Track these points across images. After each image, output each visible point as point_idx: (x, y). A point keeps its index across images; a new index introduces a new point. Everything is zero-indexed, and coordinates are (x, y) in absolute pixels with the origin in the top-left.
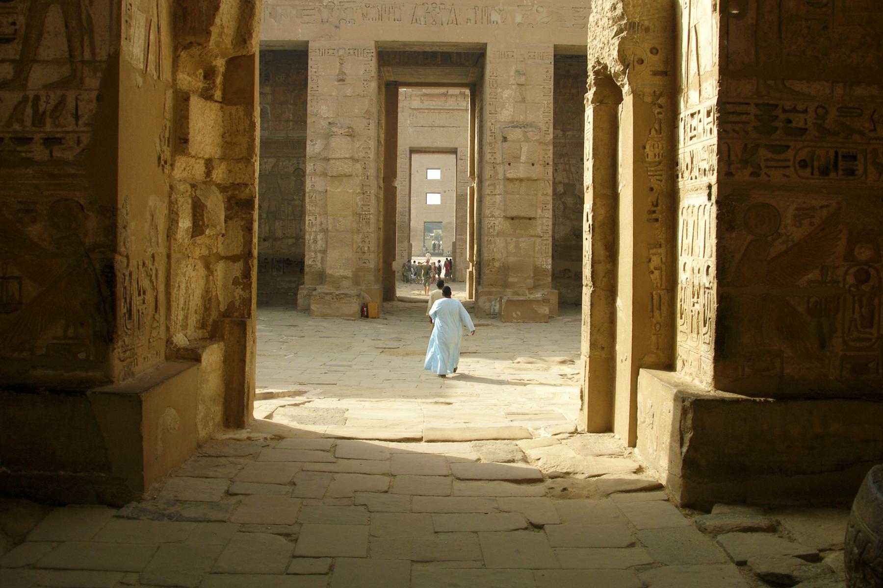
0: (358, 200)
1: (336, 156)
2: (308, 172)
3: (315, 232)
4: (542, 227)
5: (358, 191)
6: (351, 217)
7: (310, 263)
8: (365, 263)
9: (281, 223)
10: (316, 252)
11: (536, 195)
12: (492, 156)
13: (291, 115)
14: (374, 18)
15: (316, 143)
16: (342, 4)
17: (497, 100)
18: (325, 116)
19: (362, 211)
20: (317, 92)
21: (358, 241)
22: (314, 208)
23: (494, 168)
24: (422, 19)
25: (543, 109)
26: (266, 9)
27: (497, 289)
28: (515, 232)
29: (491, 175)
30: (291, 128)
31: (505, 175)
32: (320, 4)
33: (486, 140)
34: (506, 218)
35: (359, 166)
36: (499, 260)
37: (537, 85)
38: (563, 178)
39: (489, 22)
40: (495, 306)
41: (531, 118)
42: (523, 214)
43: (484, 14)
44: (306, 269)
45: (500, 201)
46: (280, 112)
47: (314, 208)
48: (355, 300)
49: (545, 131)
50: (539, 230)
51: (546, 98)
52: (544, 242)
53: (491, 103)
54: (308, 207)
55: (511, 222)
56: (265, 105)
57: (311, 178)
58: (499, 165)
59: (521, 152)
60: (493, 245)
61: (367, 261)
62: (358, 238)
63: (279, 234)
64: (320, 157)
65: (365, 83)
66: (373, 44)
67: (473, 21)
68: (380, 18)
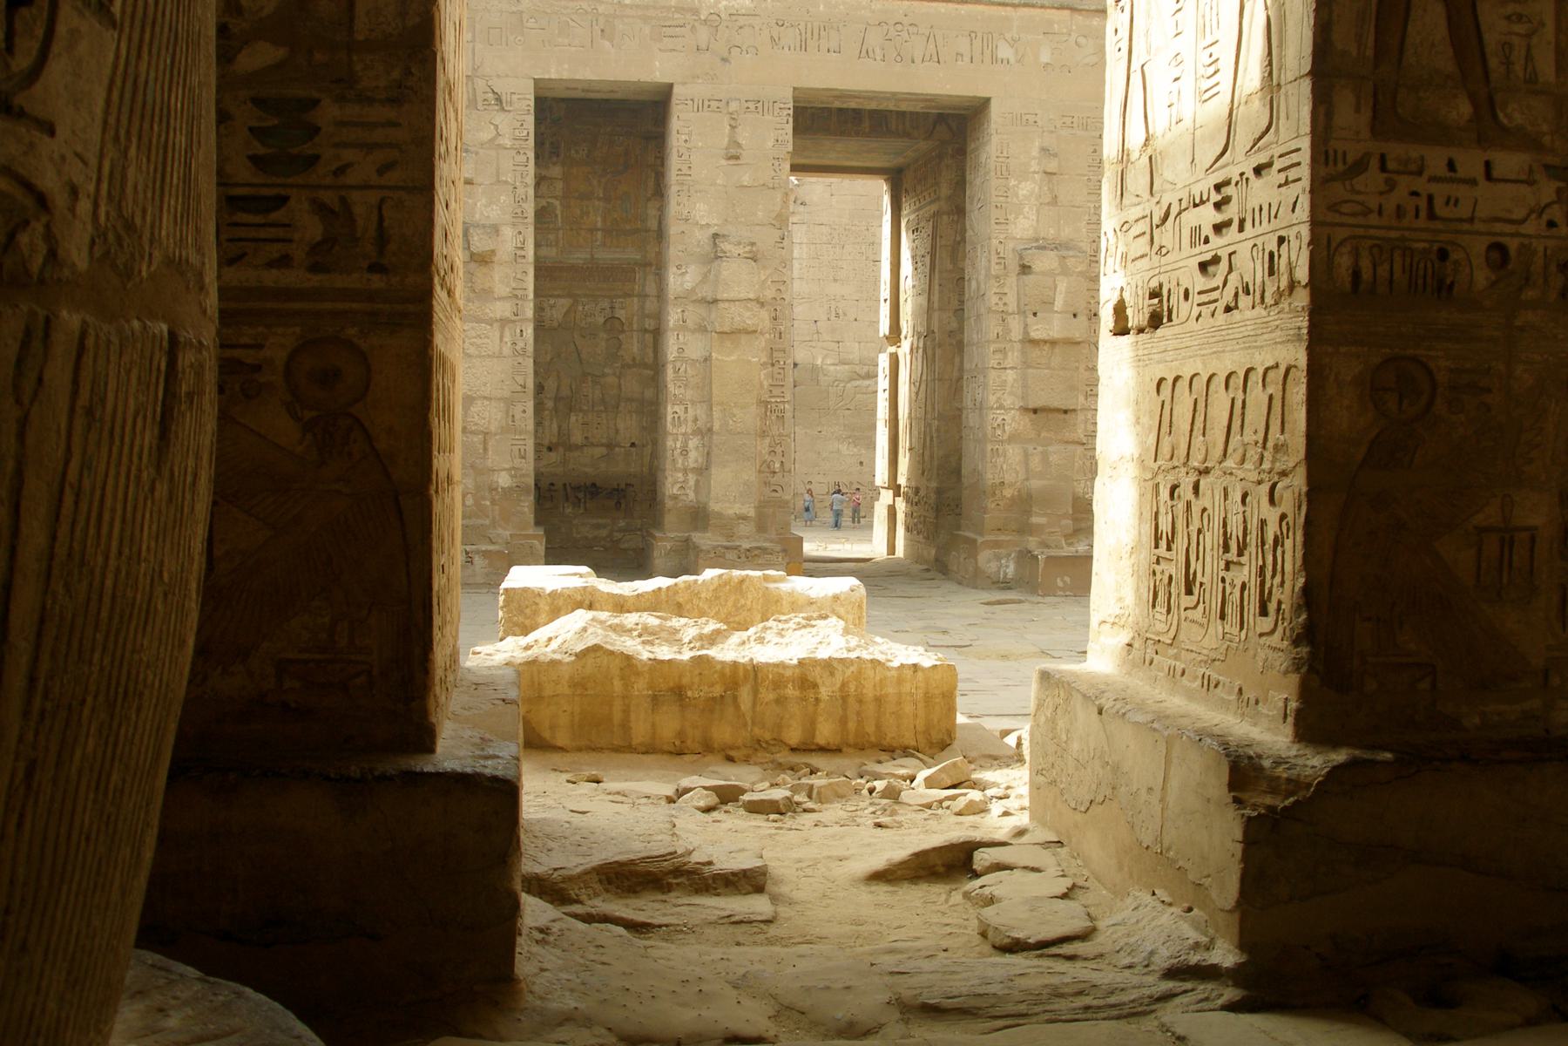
0: (762, 377)
1: (732, 295)
2: (671, 324)
3: (683, 434)
4: (1086, 427)
5: (764, 359)
7: (675, 492)
9: (580, 418)
10: (685, 471)
11: (1077, 368)
12: (1000, 299)
13: (599, 219)
15: (687, 272)
16: (734, 18)
17: (1009, 200)
18: (704, 223)
19: (771, 397)
22: (682, 390)
23: (1003, 321)
24: (878, 51)
25: (1087, 217)
26: (594, 23)
27: (1008, 538)
28: (1039, 435)
31: (1026, 332)
34: (1025, 409)
35: (765, 315)
36: (1011, 485)
37: (1078, 175)
39: (994, 59)
40: (1007, 567)
41: (1066, 233)
42: (1056, 404)
43: (985, 44)
45: (1015, 380)
46: (579, 212)
47: (682, 390)
48: (780, 559)
50: (1080, 431)
53: (999, 205)
55: (1033, 416)
56: (549, 200)
60: (1002, 459)
61: (779, 489)
63: (577, 438)
64: (695, 298)
65: (777, 163)
66: (789, 94)
67: (967, 59)
68: (804, 47)
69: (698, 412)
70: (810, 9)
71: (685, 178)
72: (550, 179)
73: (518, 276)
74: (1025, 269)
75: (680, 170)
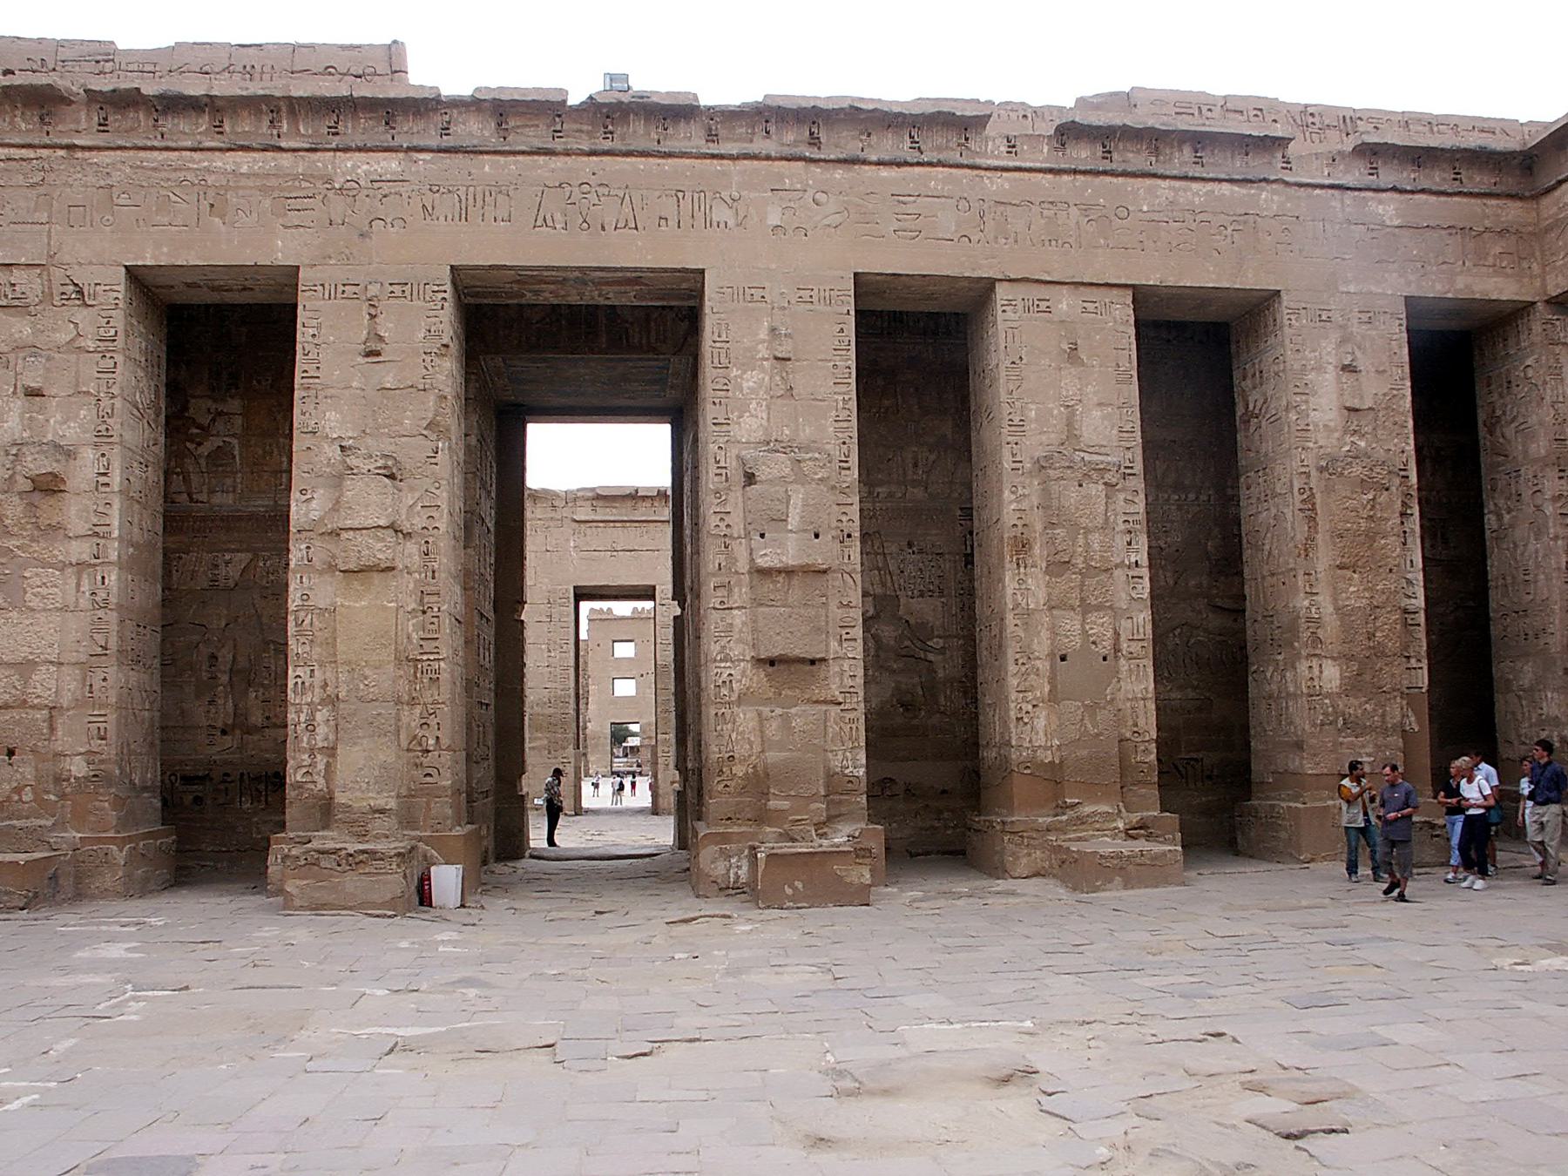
0: (411, 628)
3: (308, 704)
4: (842, 680)
5: (413, 606)
6: (391, 667)
7: (299, 778)
8: (430, 775)
9: (260, 693)
17: (730, 394)
18: (335, 436)
20: (317, 381)
21: (413, 724)
24: (558, 216)
25: (834, 413)
27: (743, 829)
29: (720, 565)
33: (707, 483)
34: (759, 661)
35: (412, 548)
37: (820, 360)
38: (872, 585)
39: (708, 223)
40: (739, 867)
42: (797, 652)
43: (696, 207)
44: (290, 793)
45: (744, 623)
46: (260, 452)
48: (394, 867)
49: (841, 461)
50: (834, 687)
51: (843, 388)
52: (848, 715)
53: (717, 401)
55: (770, 669)
56: (226, 439)
57: (301, 577)
58: (738, 541)
59: (788, 507)
60: (729, 726)
62: (411, 717)
65: (428, 359)
67: (673, 223)
69: (328, 674)
70: (473, 171)
71: (311, 381)
72: (226, 414)
73: (101, 509)
74: (750, 479)
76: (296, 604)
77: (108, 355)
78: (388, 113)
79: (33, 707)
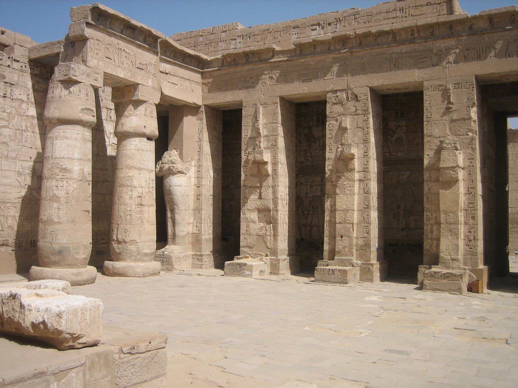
3: (431, 224)
7: (428, 247)
10: (432, 239)
14: (474, 58)
16: (448, 51)
19: (468, 208)
20: (431, 118)
22: (430, 206)
26: (391, 62)
30: (420, 149)
32: (432, 53)
44: (425, 252)
47: (430, 206)
54: (426, 205)
56: (401, 134)
57: (428, 183)
61: (473, 247)
71: (429, 119)
75: (427, 116)
76: (426, 192)
77: (366, 115)
78: (450, 25)
79: (348, 223)
